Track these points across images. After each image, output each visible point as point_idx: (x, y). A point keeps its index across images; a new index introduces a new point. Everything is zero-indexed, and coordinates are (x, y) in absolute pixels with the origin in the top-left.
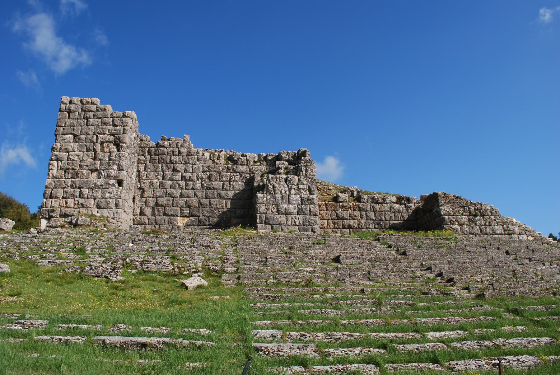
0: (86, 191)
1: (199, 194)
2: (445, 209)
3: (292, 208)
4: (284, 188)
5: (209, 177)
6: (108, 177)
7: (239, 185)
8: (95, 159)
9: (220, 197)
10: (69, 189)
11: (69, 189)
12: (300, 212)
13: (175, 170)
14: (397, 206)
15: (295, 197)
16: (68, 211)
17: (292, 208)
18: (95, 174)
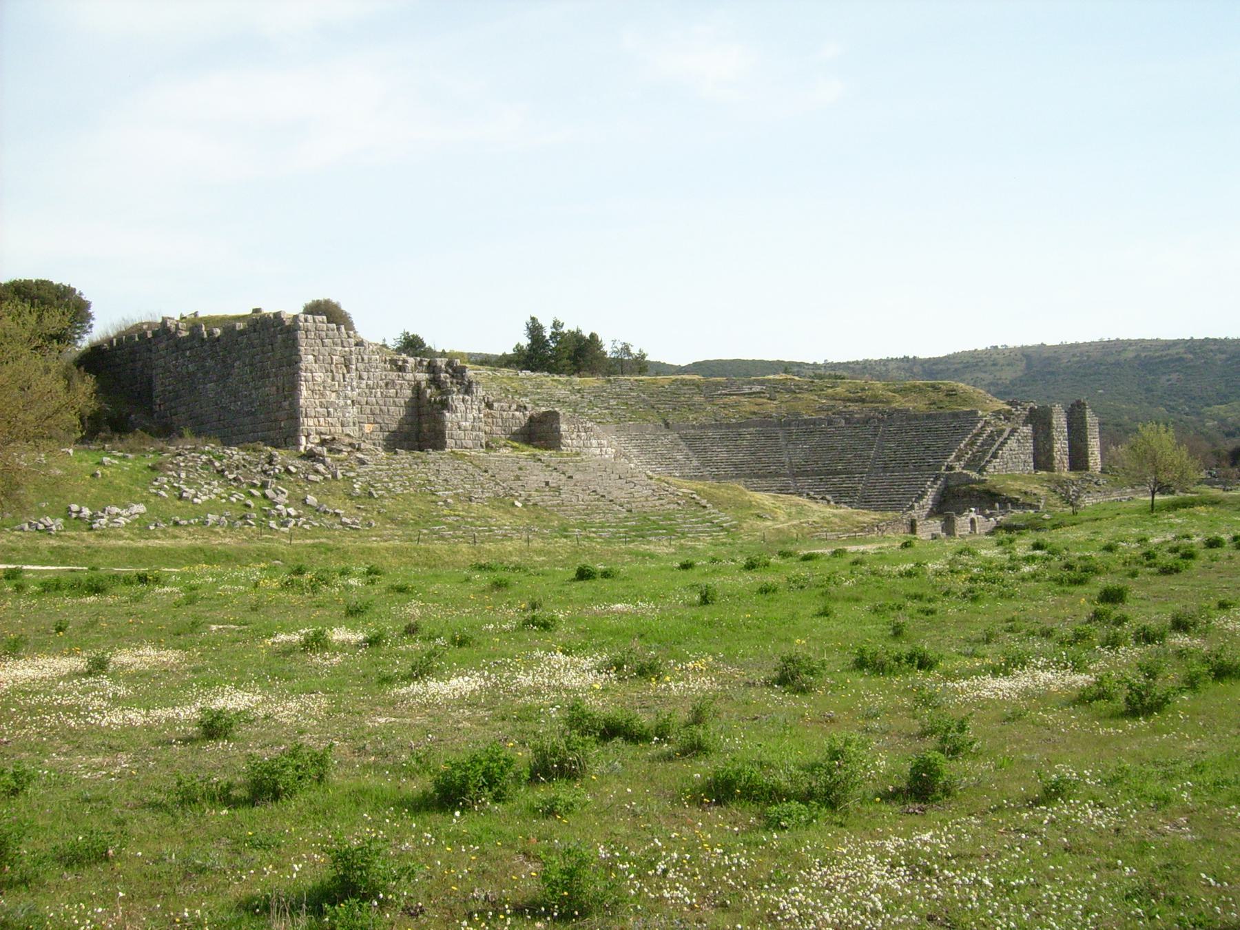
0: (331, 410)
1: (381, 402)
2: (563, 427)
3: (467, 425)
4: (461, 407)
5: (387, 384)
6: (346, 397)
7: (408, 393)
8: (333, 380)
9: (395, 404)
10: (319, 409)
11: (319, 409)
12: (473, 428)
13: (360, 378)
14: (517, 413)
15: (470, 416)
16: (323, 429)
17: (467, 425)
18: (334, 395)
